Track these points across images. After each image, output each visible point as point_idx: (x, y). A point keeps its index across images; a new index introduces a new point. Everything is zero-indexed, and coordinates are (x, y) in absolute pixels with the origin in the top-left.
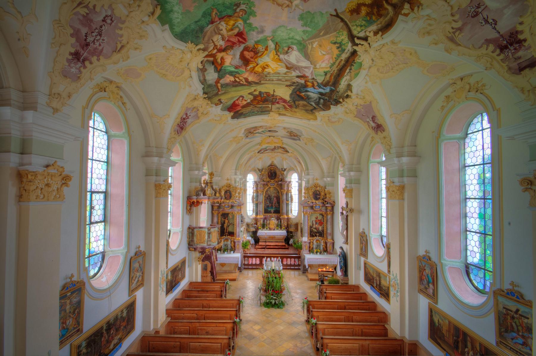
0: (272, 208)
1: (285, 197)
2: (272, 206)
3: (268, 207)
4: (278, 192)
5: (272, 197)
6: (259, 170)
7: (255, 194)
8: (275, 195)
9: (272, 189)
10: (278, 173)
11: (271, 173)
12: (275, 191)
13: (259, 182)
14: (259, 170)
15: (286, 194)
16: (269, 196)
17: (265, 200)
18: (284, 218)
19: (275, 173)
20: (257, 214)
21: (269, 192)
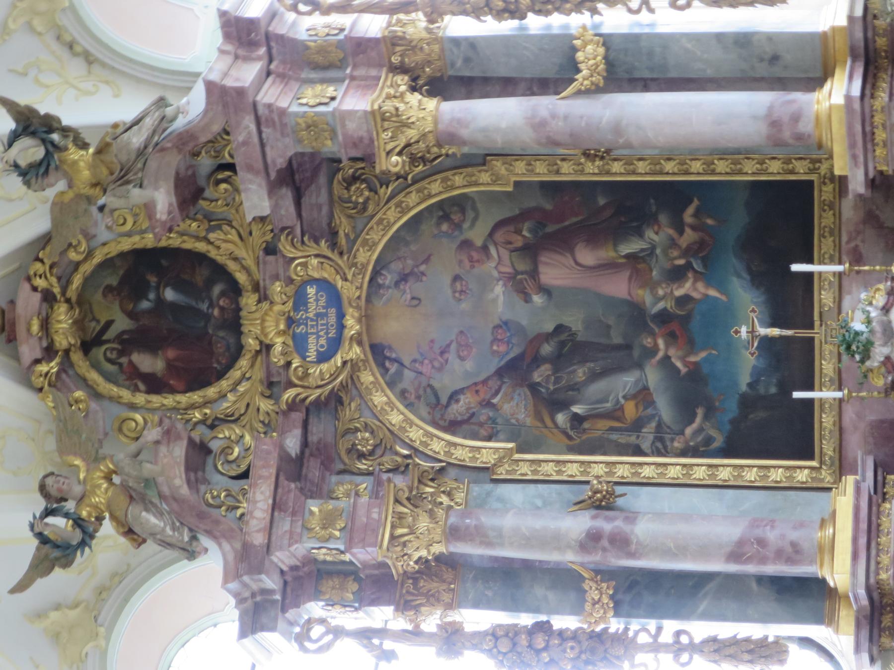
0: (721, 318)
1: (496, 116)
2: (677, 324)
3: (693, 391)
4: (452, 211)
5: (536, 316)
6: (54, 553)
7: (477, 619)
8: (498, 262)
9: (398, 326)
10: (113, 238)
11: (141, 339)
12: (439, 276)
13: (247, 561)
14: (54, 553)
15: (441, 86)
16: (515, 370)
17: (582, 438)
18: (864, 122)
19: (140, 269)
20: (805, 595)
21: (457, 372)
